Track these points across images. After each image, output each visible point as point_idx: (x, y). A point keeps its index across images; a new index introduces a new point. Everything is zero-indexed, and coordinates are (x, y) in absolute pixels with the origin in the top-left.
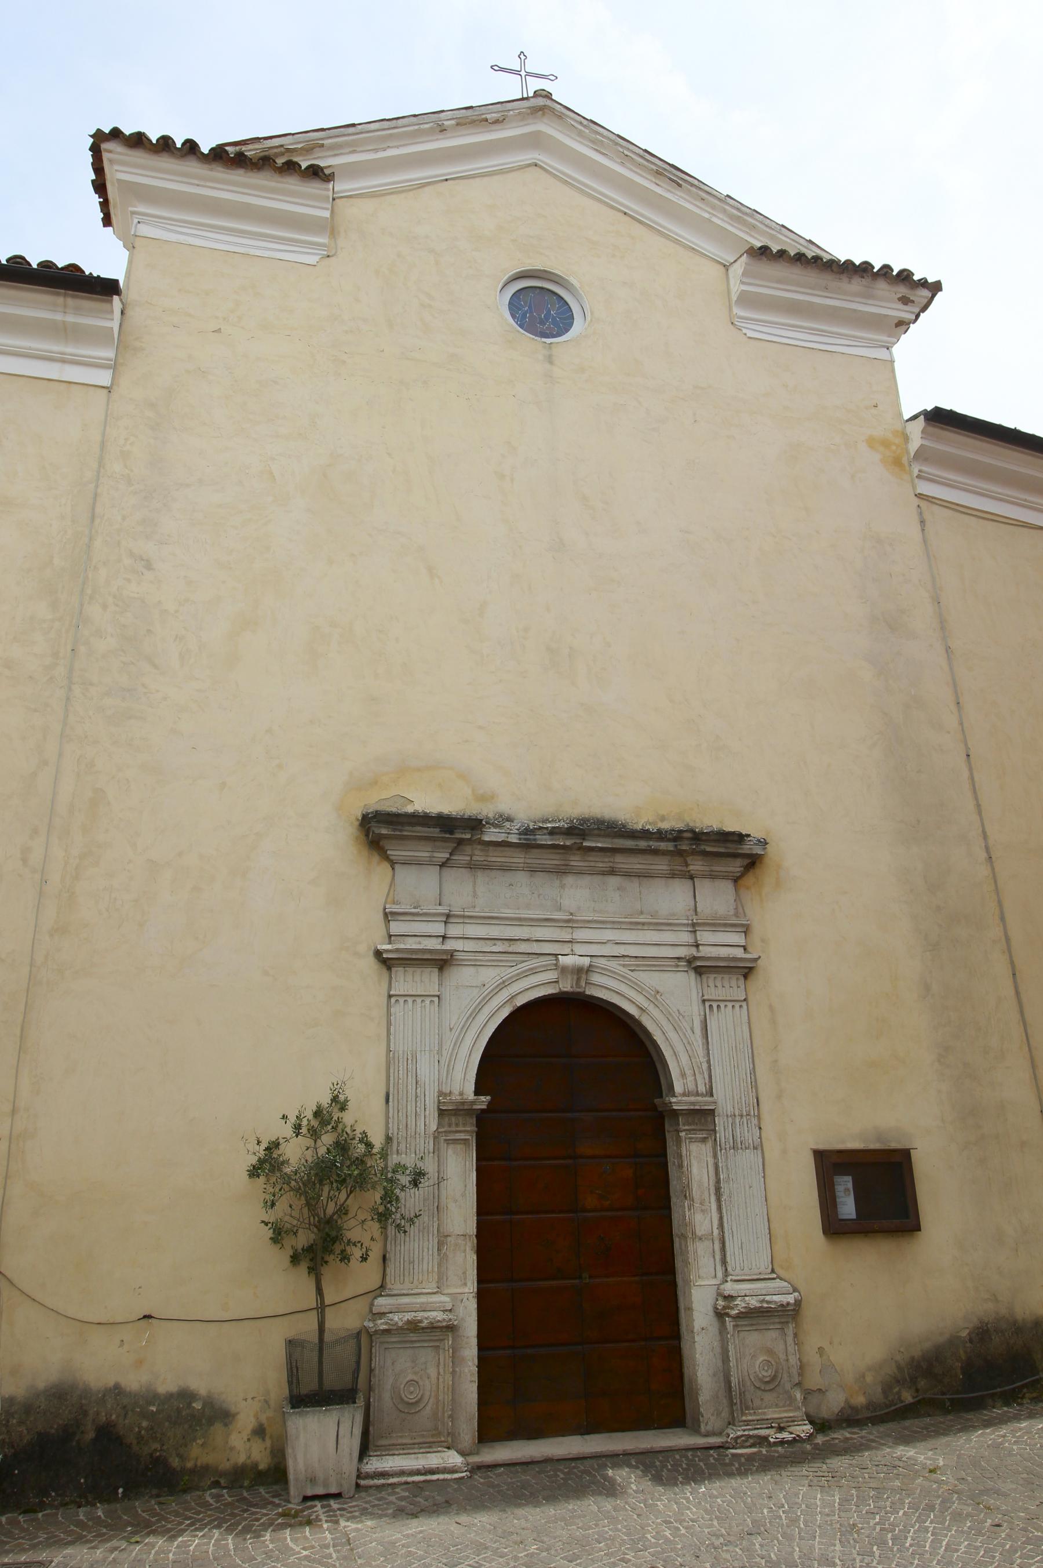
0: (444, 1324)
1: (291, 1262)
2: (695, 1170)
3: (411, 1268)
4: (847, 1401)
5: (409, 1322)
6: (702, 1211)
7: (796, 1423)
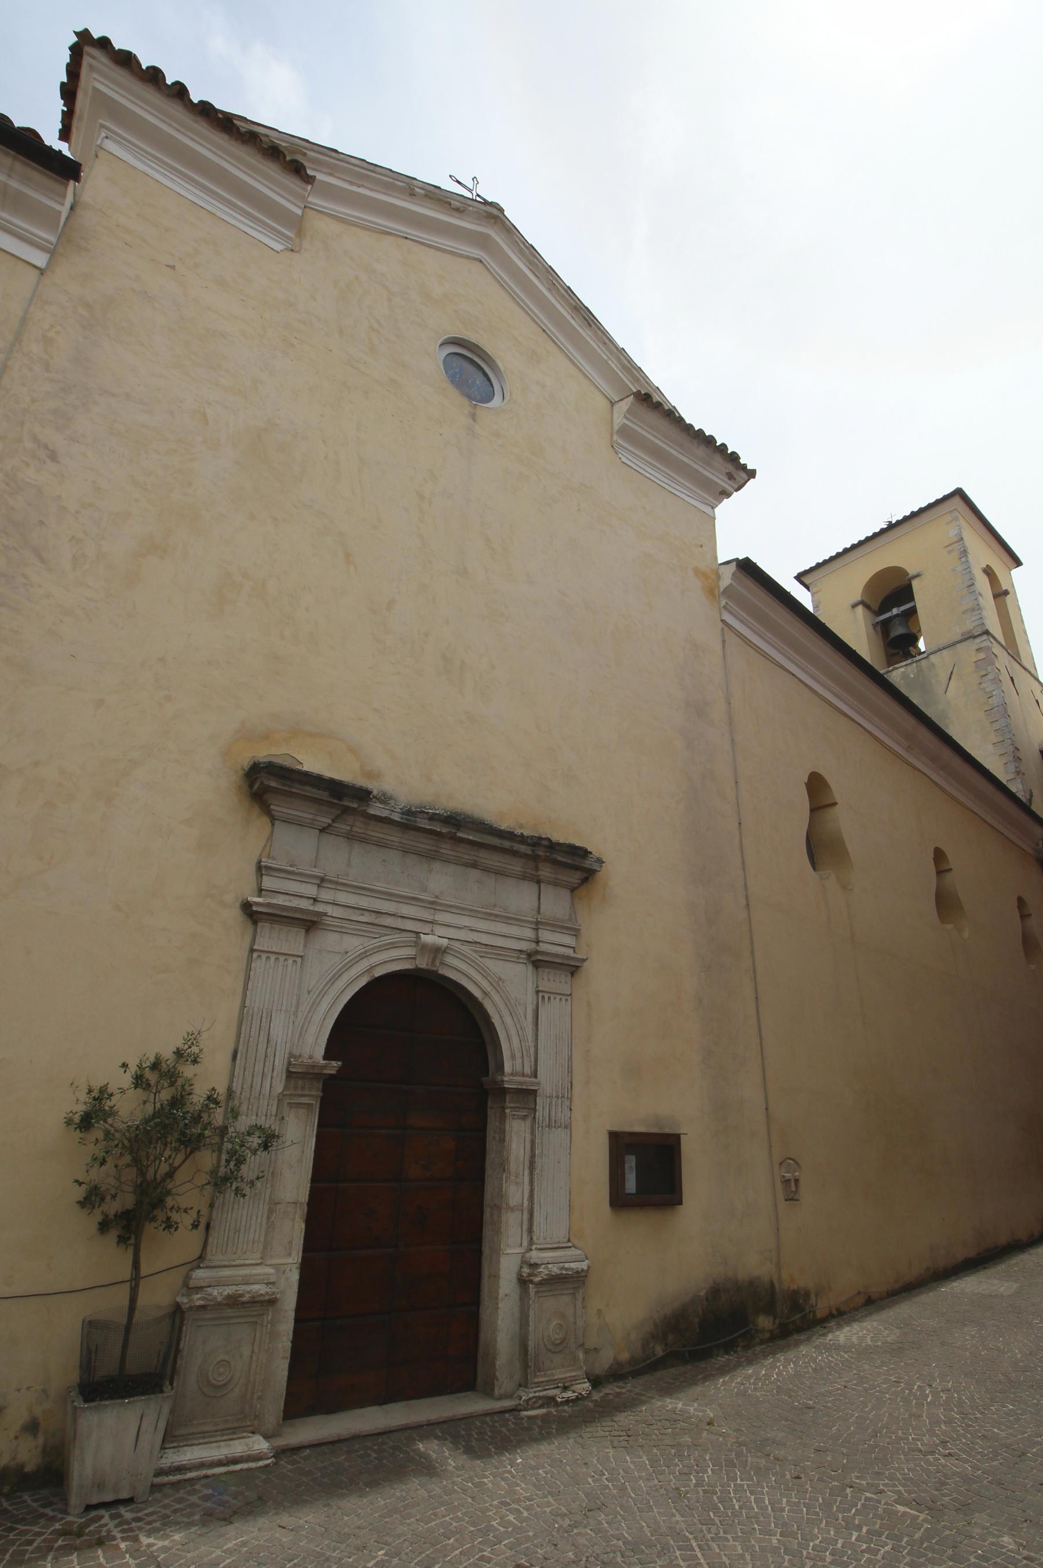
0: (267, 1298)
1: (99, 1229)
2: (514, 1146)
3: (237, 1236)
4: (615, 1358)
5: (229, 1296)
6: (517, 1183)
7: (578, 1382)
